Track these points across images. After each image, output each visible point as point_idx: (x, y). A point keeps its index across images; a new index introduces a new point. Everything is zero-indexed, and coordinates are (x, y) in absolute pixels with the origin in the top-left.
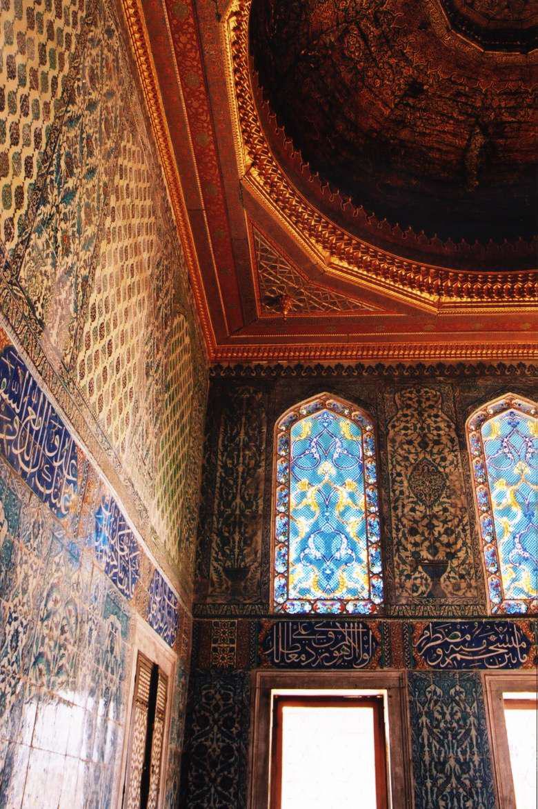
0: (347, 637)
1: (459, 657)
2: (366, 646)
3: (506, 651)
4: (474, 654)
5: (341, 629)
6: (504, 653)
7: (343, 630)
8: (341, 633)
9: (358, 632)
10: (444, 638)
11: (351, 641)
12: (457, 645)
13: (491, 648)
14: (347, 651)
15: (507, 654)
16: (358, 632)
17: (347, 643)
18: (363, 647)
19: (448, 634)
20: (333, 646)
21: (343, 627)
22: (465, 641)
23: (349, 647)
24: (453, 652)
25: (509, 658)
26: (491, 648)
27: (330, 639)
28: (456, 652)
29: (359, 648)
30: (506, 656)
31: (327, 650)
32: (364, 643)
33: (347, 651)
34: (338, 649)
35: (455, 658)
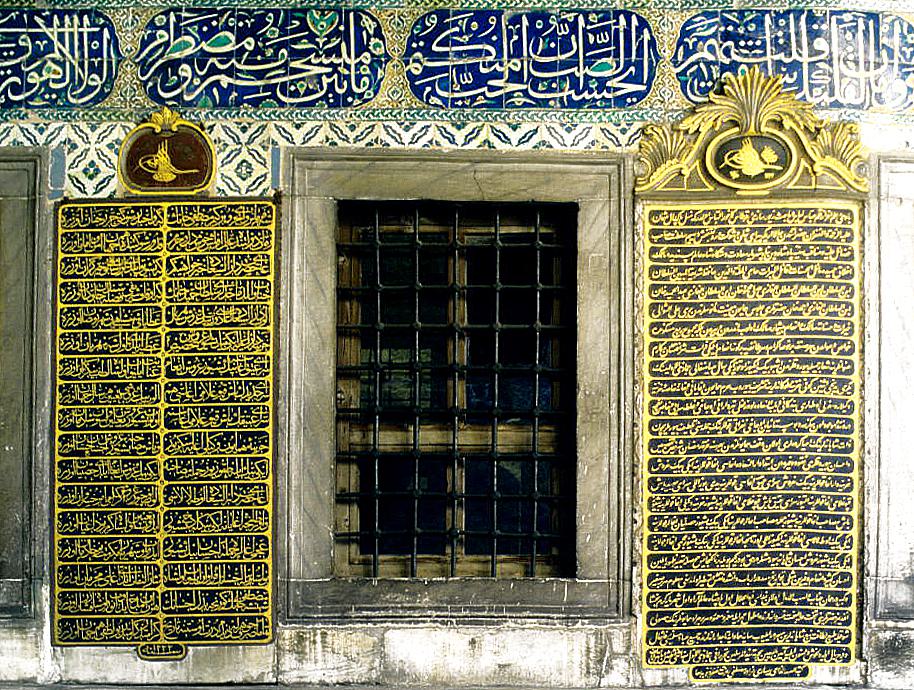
0: (57, 44)
1: (225, 81)
2: (96, 61)
3: (330, 70)
4: (260, 75)
5: (44, 29)
6: (319, 76)
7: (48, 31)
8: (42, 36)
9: (81, 34)
10: (197, 44)
11: (66, 51)
12: (225, 57)
13: (294, 64)
14: (55, 72)
15: (329, 75)
16: (81, 34)
17: (57, 55)
18: (91, 64)
19: (205, 37)
20: (29, 63)
21: (49, 24)
22: (242, 50)
23: (62, 64)
24: (214, 70)
25: (331, 86)
26: (294, 64)
27: (24, 50)
28: (220, 72)
29: (81, 65)
30: (325, 81)
31: (16, 70)
32: (92, 53)
33: (55, 72)
34: (39, 70)
35: (217, 83)
